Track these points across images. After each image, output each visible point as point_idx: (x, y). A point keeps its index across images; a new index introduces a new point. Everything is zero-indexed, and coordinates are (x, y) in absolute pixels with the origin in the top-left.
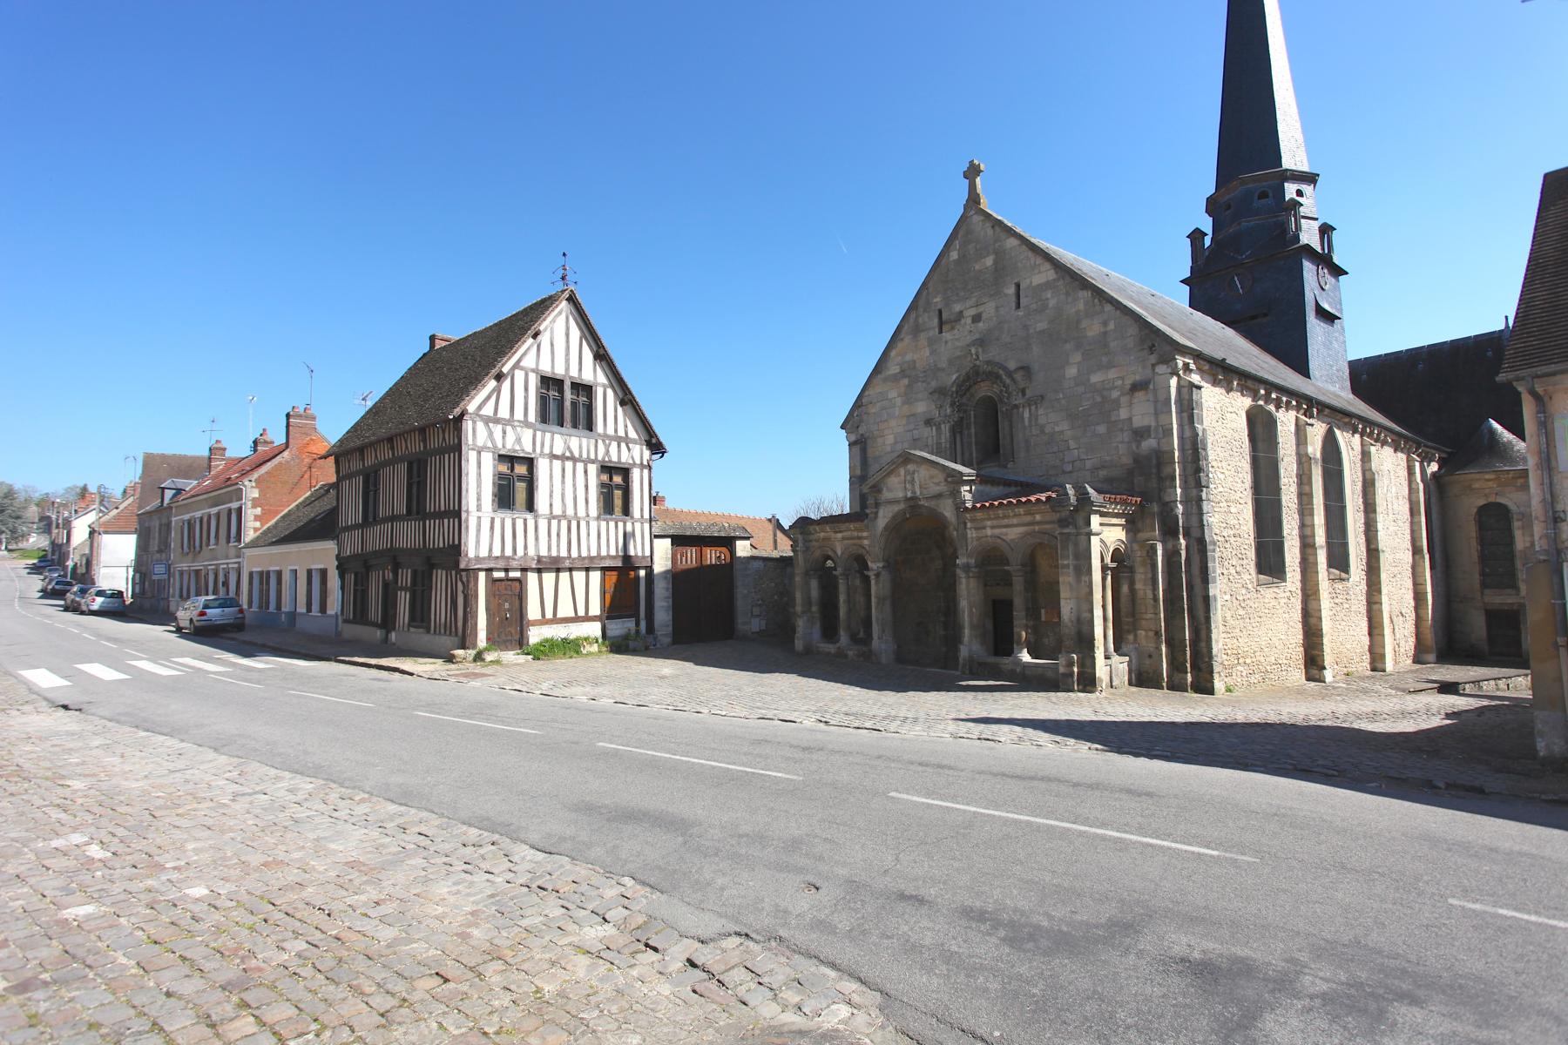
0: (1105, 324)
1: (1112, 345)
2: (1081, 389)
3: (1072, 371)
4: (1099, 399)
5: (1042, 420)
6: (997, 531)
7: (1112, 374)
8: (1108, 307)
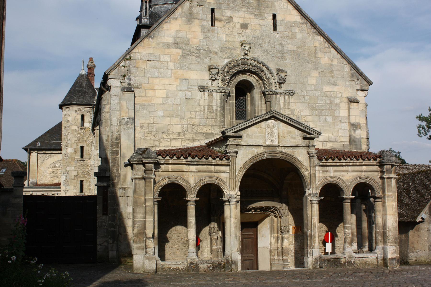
0: (332, 60)
1: (336, 73)
2: (317, 93)
3: (312, 81)
4: (328, 102)
5: (292, 106)
6: (337, 174)
7: (336, 89)
8: (333, 50)
